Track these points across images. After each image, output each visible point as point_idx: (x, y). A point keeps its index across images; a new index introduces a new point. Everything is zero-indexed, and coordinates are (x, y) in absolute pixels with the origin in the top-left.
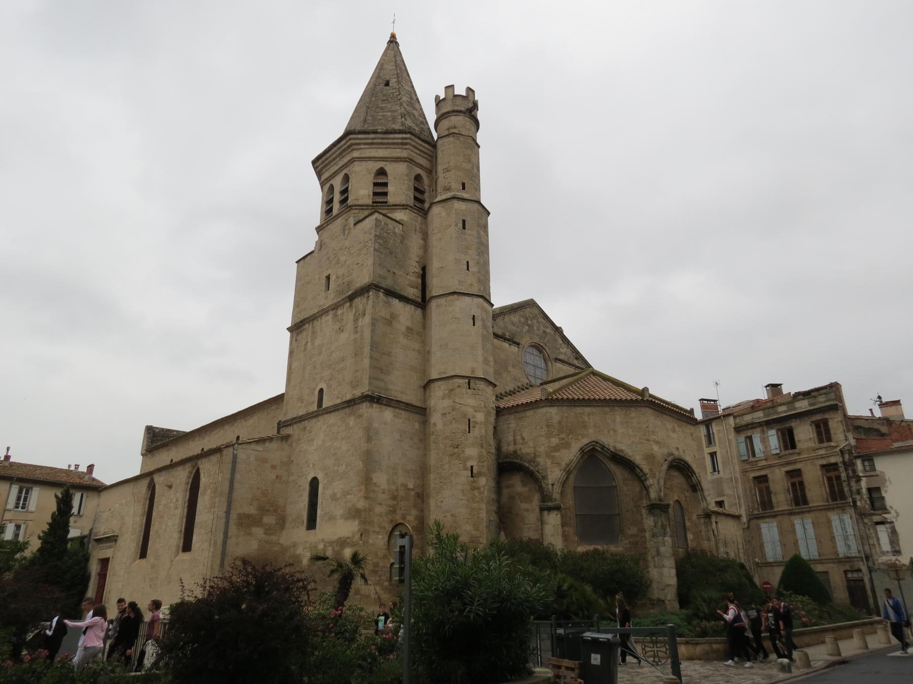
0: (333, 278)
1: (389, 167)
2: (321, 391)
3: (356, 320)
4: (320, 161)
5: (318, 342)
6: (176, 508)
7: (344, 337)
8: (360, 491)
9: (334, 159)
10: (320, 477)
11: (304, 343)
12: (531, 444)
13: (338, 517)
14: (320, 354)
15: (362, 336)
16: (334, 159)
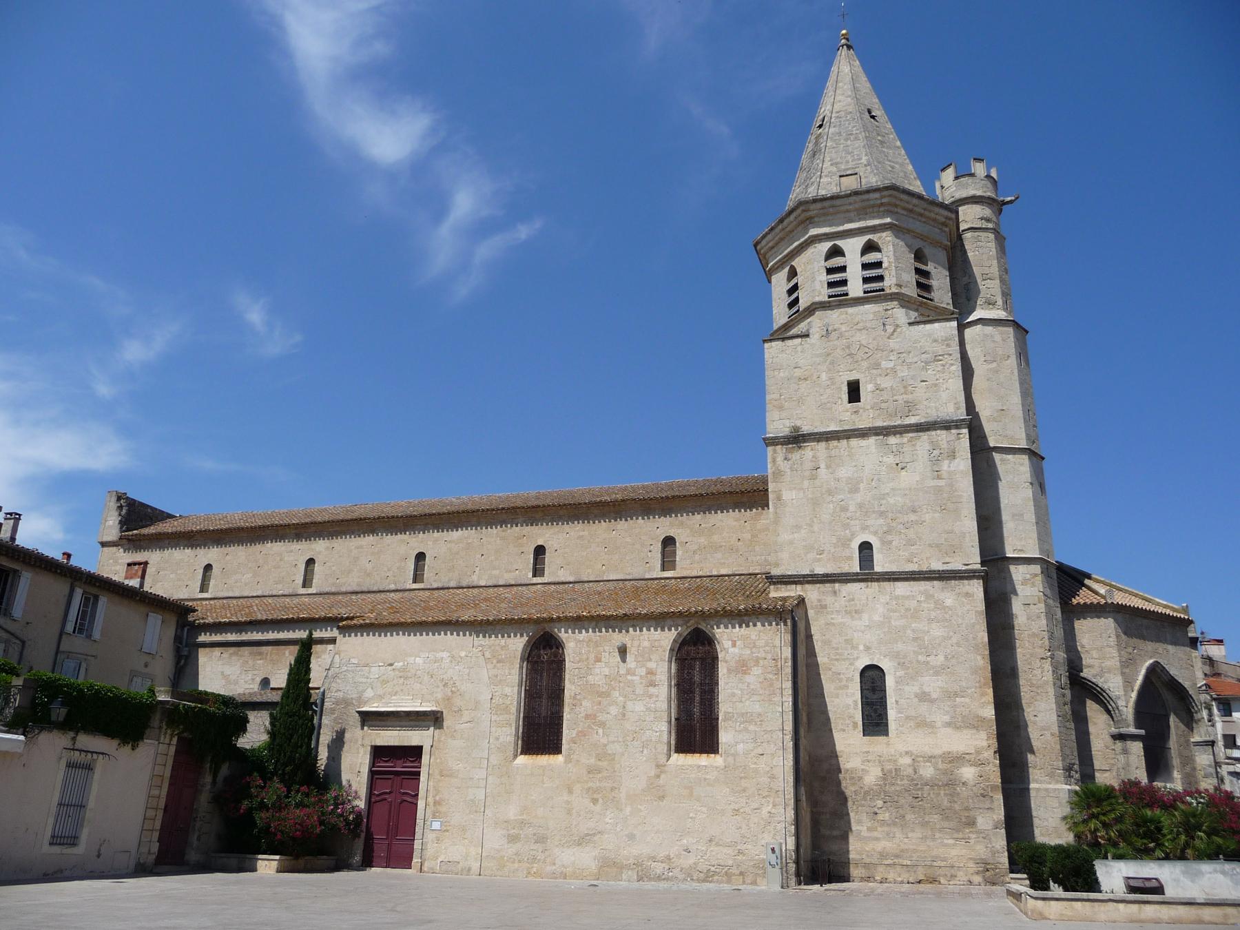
0: (866, 390)
2: (866, 547)
4: (819, 205)
5: (844, 472)
6: (652, 684)
7: (907, 479)
8: (983, 695)
9: (848, 211)
10: (885, 665)
11: (808, 465)
12: (1095, 654)
13: (939, 724)
14: (855, 490)
15: (951, 485)
16: (848, 211)
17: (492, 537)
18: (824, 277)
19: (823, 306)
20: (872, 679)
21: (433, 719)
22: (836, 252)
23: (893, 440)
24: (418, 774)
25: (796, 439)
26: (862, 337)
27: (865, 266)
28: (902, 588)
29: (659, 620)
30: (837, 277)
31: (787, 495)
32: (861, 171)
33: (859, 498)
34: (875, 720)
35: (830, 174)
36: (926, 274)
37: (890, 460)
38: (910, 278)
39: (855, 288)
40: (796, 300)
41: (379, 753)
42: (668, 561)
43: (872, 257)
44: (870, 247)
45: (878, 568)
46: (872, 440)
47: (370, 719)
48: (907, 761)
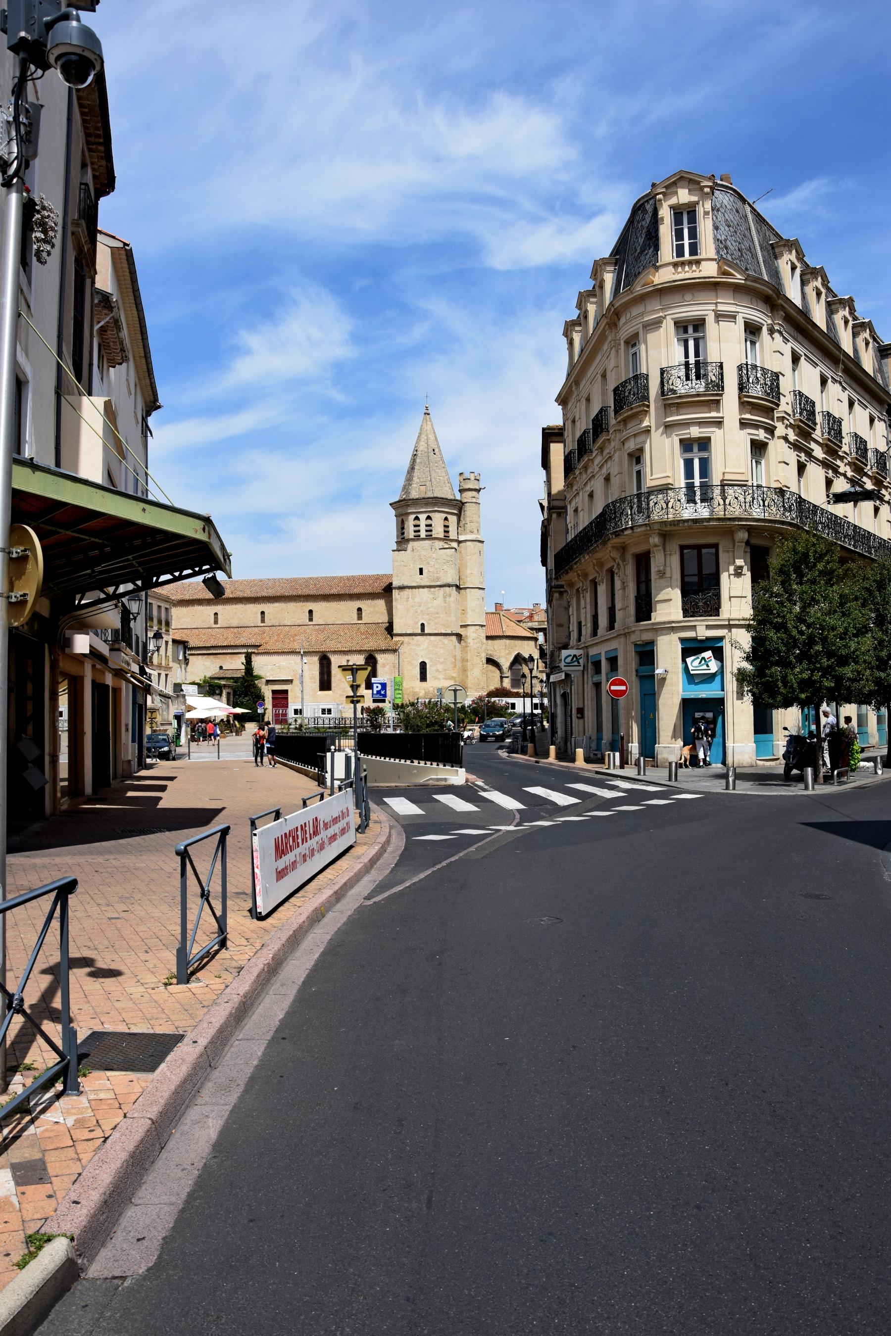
1: (449, 517)
2: (423, 625)
3: (445, 597)
5: (417, 600)
7: (436, 603)
14: (420, 606)
17: (291, 606)
18: (412, 528)
19: (412, 540)
20: (423, 666)
21: (290, 681)
22: (417, 518)
23: (432, 590)
24: (287, 698)
25: (402, 588)
26: (423, 553)
27: (427, 526)
28: (433, 638)
29: (360, 652)
30: (417, 528)
31: (399, 607)
32: (428, 483)
33: (421, 608)
34: (423, 677)
35: (417, 483)
36: (448, 527)
37: (432, 596)
38: (441, 529)
39: (423, 534)
40: (403, 534)
41: (274, 692)
42: (360, 617)
43: (429, 522)
44: (429, 518)
45: (426, 632)
46: (426, 590)
47: (268, 682)
48: (431, 689)
